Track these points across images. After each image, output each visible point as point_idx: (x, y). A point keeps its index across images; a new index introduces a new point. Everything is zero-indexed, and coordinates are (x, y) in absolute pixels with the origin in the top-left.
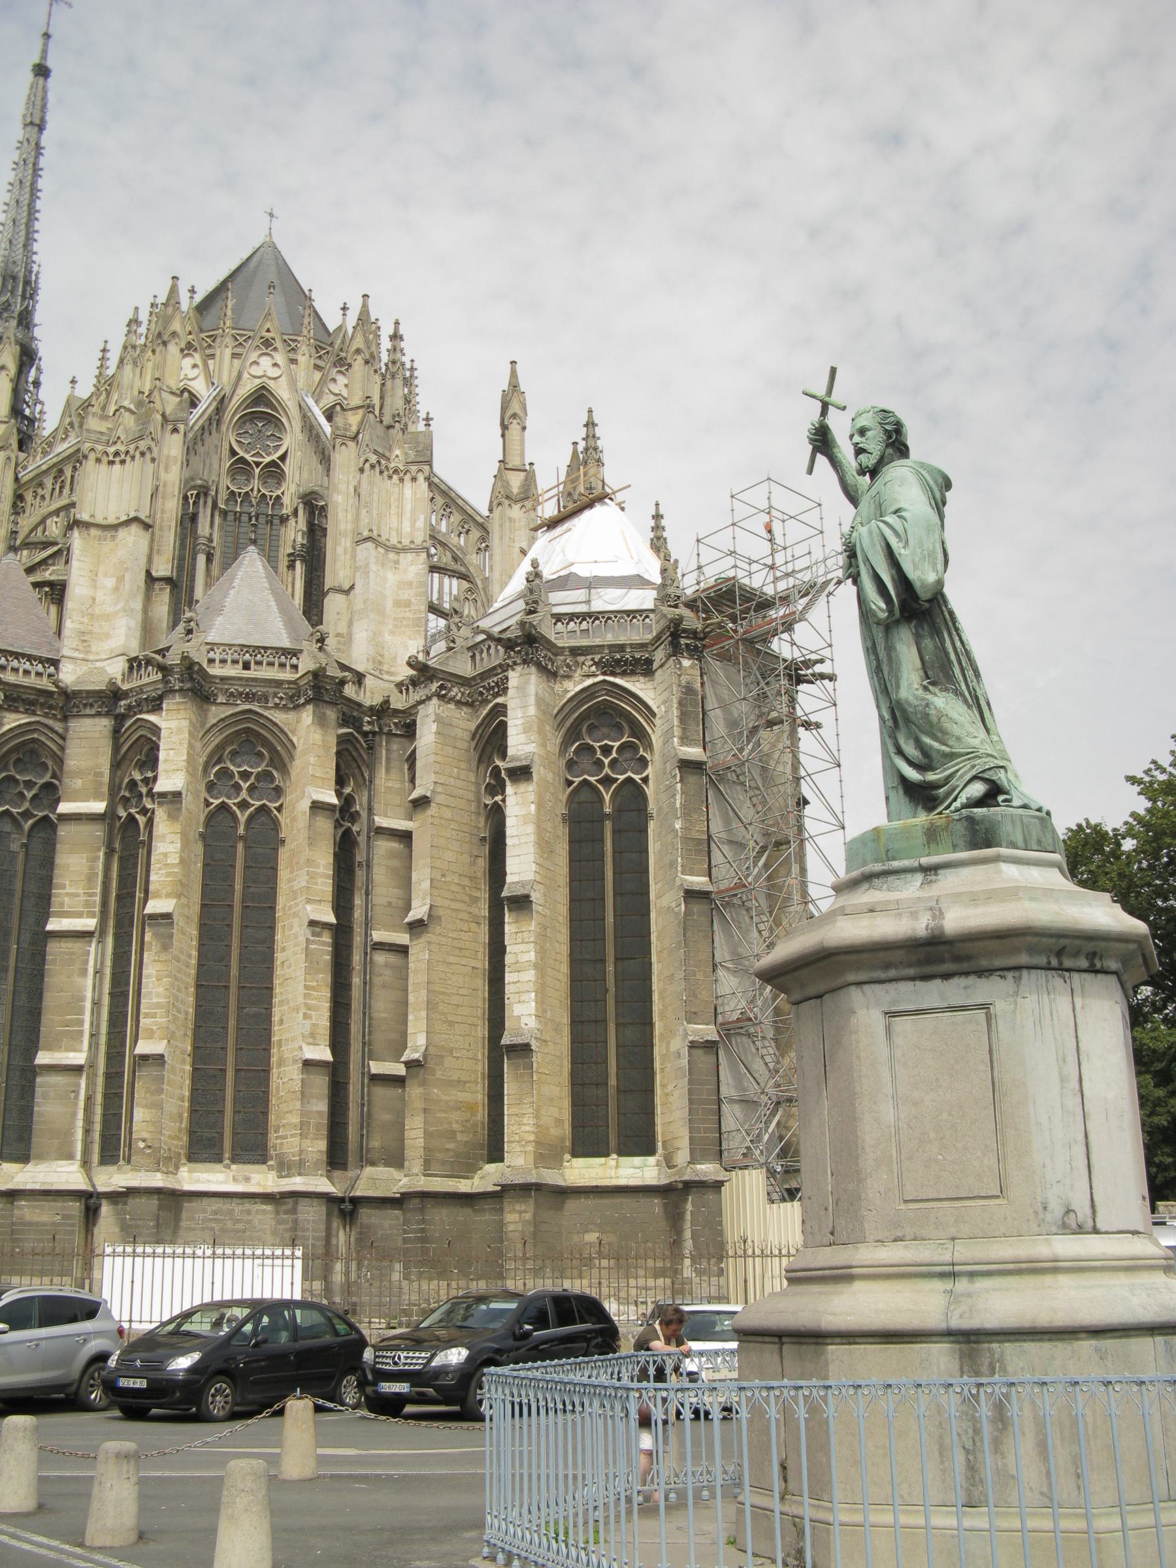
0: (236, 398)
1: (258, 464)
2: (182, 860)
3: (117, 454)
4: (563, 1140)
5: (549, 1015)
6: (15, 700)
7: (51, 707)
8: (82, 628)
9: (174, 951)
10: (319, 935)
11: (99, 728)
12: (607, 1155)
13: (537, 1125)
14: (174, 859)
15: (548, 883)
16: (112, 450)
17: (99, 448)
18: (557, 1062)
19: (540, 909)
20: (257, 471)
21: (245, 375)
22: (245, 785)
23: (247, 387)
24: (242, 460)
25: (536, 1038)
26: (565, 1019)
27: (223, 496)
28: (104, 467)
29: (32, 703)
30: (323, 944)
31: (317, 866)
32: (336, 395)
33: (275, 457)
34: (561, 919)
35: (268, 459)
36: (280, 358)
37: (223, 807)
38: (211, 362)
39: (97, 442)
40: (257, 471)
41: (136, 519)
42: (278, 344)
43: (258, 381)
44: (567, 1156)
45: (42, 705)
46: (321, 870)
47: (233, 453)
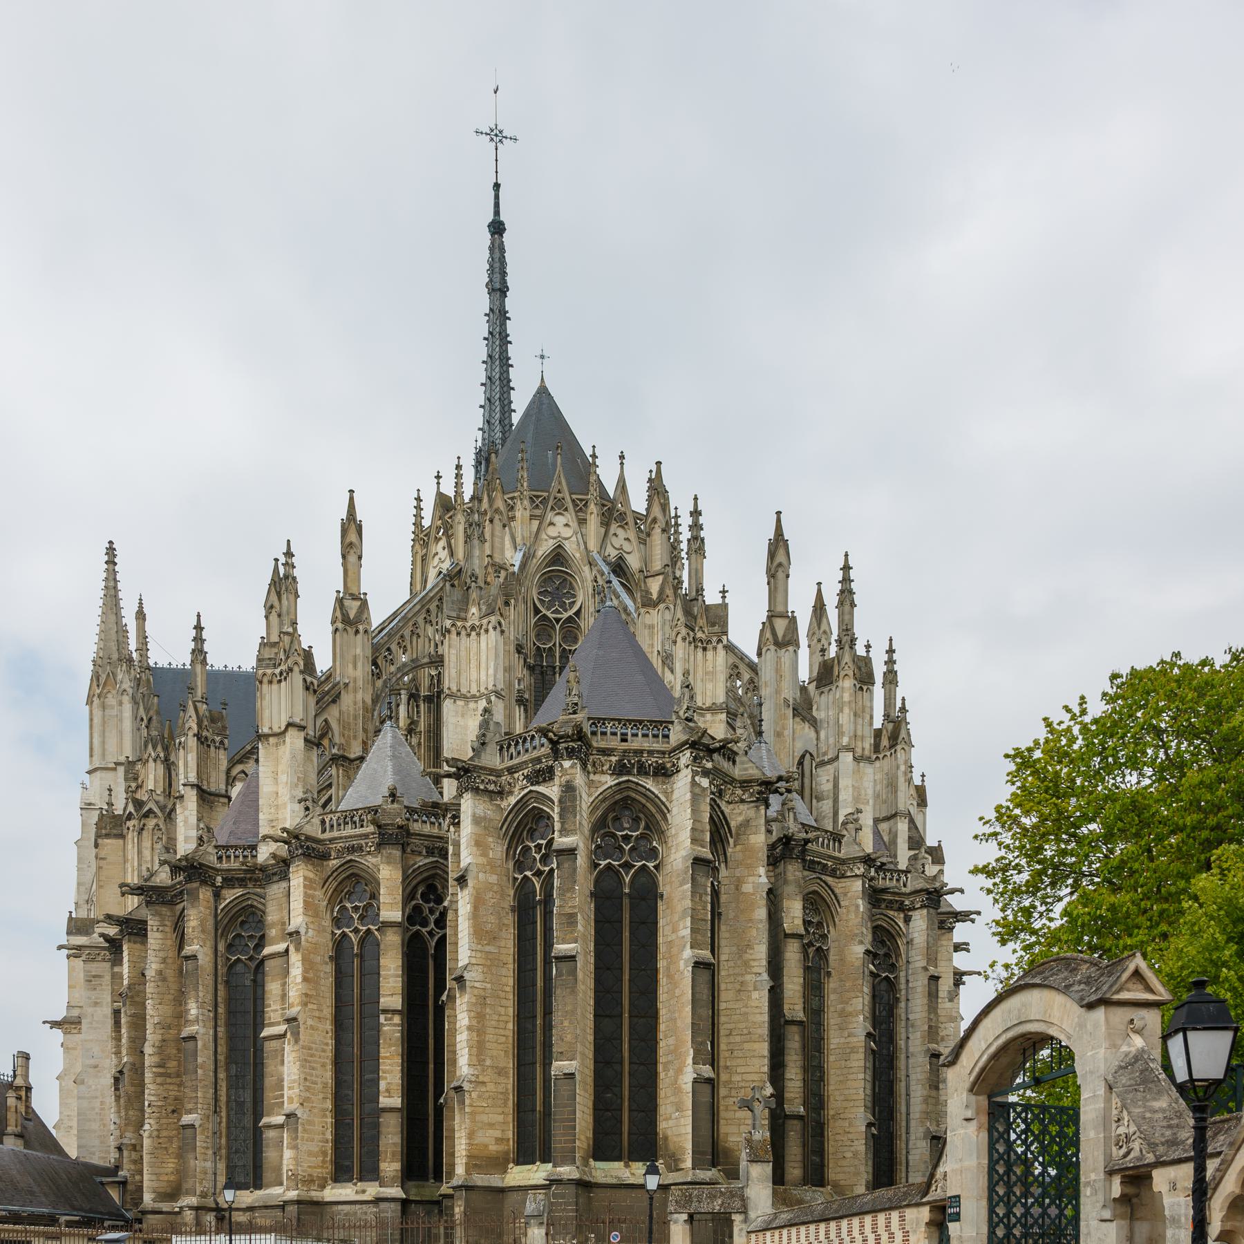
2: (305, 979)
4: (507, 1153)
5: (488, 1062)
6: (231, 880)
7: (256, 880)
8: (271, 818)
9: (301, 1043)
10: (391, 1019)
11: (281, 890)
12: (534, 1163)
13: (470, 1144)
14: (299, 979)
15: (489, 963)
18: (501, 1096)
19: (477, 985)
22: (356, 916)
25: (470, 1082)
26: (509, 1064)
29: (243, 880)
30: (395, 1025)
31: (390, 970)
34: (508, 989)
37: (344, 935)
44: (511, 1165)
45: (250, 879)
46: (392, 972)
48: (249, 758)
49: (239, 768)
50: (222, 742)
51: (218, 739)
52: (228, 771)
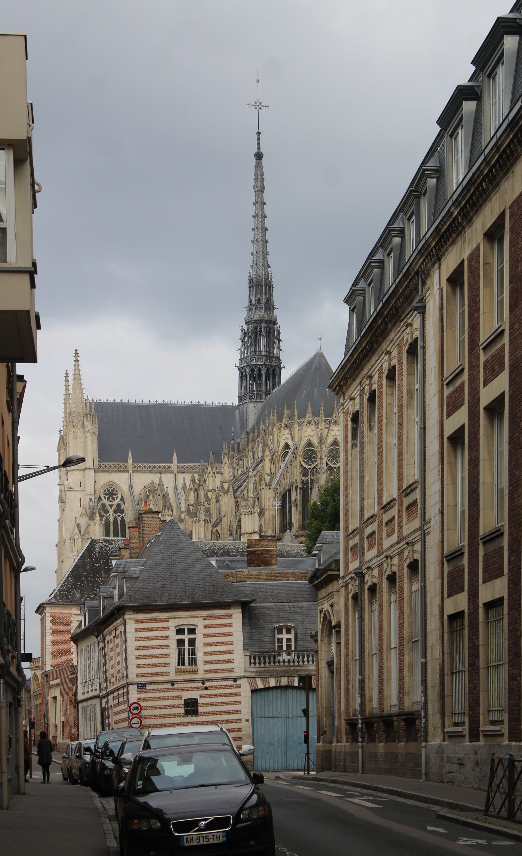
0: (301, 446)
1: (310, 469)
3: (249, 512)
16: (248, 511)
17: (245, 511)
20: (310, 471)
21: (303, 437)
23: (304, 442)
24: (305, 468)
27: (300, 482)
28: (247, 516)
32: (334, 436)
33: (314, 465)
35: (312, 467)
36: (313, 427)
38: (292, 432)
39: (244, 509)
40: (310, 471)
41: (255, 532)
42: (313, 423)
43: (307, 438)
47: (302, 466)
48: (218, 525)
49: (215, 529)
50: (210, 520)
51: (208, 519)
52: (212, 532)
